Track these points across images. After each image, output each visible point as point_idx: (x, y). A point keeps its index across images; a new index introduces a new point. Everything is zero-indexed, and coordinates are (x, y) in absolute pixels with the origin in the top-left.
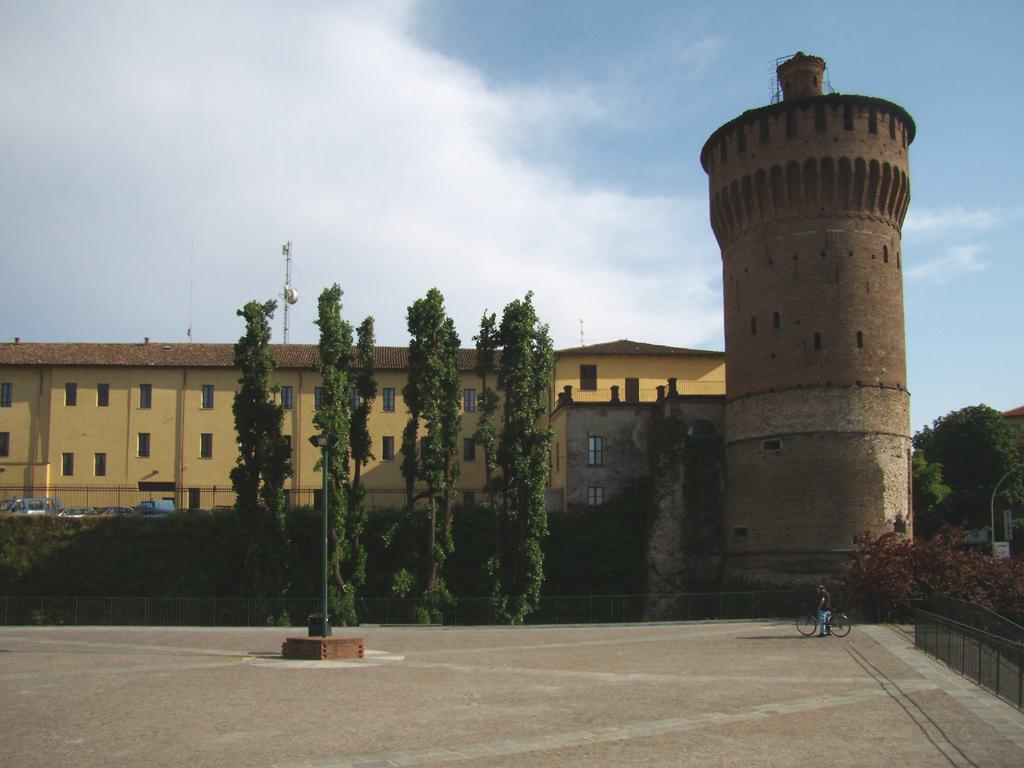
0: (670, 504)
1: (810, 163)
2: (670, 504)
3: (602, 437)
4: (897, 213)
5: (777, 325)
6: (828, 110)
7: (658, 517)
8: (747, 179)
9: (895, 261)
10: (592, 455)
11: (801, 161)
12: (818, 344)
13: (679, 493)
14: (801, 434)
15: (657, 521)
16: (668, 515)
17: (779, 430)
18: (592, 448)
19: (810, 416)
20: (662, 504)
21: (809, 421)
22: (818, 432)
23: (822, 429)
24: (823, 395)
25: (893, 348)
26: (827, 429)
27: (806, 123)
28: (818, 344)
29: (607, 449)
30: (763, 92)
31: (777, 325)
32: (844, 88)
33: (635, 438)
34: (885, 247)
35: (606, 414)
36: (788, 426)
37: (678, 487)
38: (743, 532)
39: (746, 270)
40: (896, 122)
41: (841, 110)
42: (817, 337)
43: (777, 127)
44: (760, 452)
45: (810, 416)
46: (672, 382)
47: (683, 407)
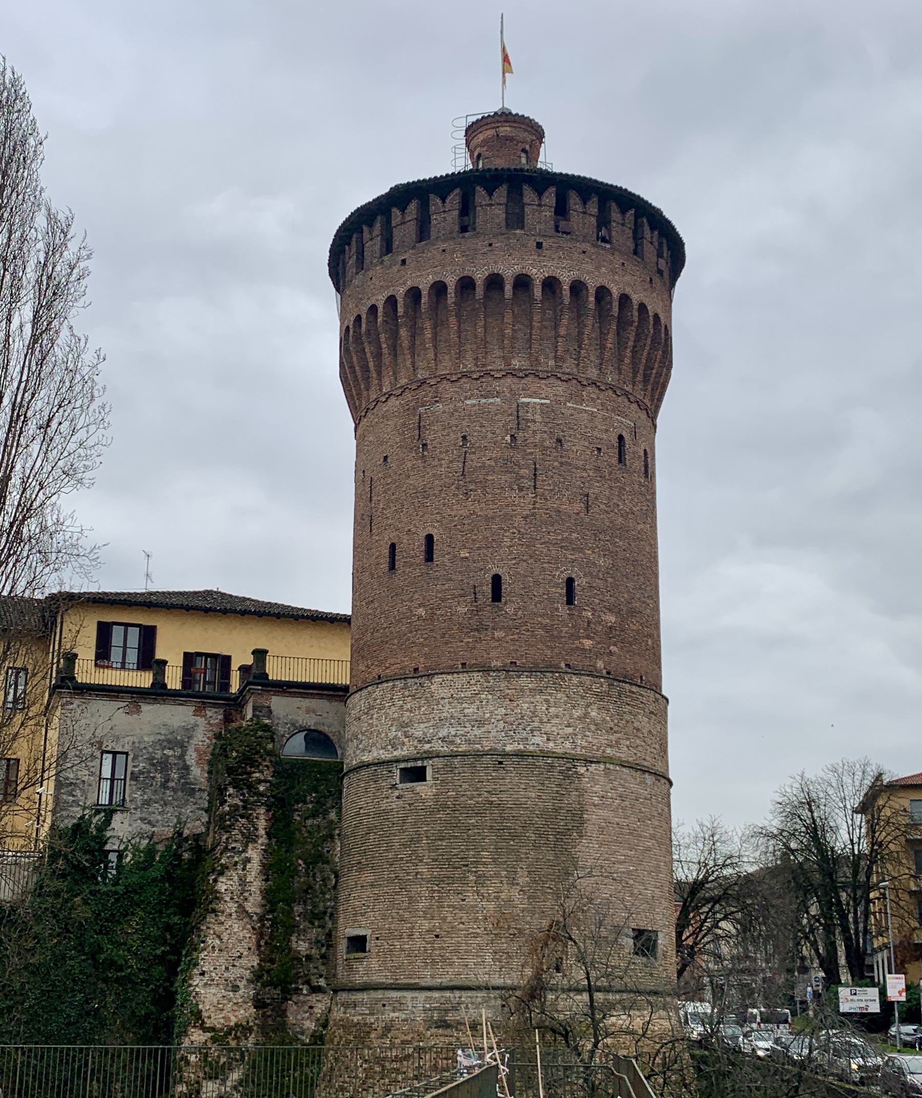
0: (240, 883)
1: (495, 282)
2: (240, 883)
3: (127, 754)
4: (646, 380)
5: (429, 557)
6: (529, 195)
7: (214, 911)
8: (391, 301)
9: (638, 465)
10: (106, 786)
11: (480, 277)
12: (497, 595)
13: (255, 866)
14: (464, 755)
15: (210, 918)
16: (232, 907)
17: (427, 746)
18: (107, 773)
19: (481, 723)
20: (222, 887)
21: (477, 732)
22: (492, 753)
23: (499, 747)
24: (503, 685)
25: (632, 612)
26: (509, 748)
27: (491, 209)
28: (497, 595)
29: (134, 777)
30: (450, 158)
31: (429, 557)
32: (558, 168)
33: (191, 758)
34: (621, 438)
35: (138, 711)
36: (443, 739)
37: (254, 854)
38: (358, 944)
39: (386, 458)
40: (647, 229)
41: (550, 198)
42: (497, 580)
43: (444, 216)
44: (394, 787)
45: (481, 723)
46: (260, 655)
47: (280, 705)
